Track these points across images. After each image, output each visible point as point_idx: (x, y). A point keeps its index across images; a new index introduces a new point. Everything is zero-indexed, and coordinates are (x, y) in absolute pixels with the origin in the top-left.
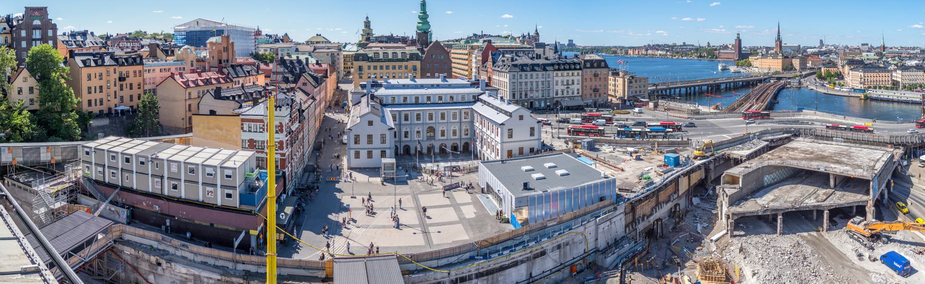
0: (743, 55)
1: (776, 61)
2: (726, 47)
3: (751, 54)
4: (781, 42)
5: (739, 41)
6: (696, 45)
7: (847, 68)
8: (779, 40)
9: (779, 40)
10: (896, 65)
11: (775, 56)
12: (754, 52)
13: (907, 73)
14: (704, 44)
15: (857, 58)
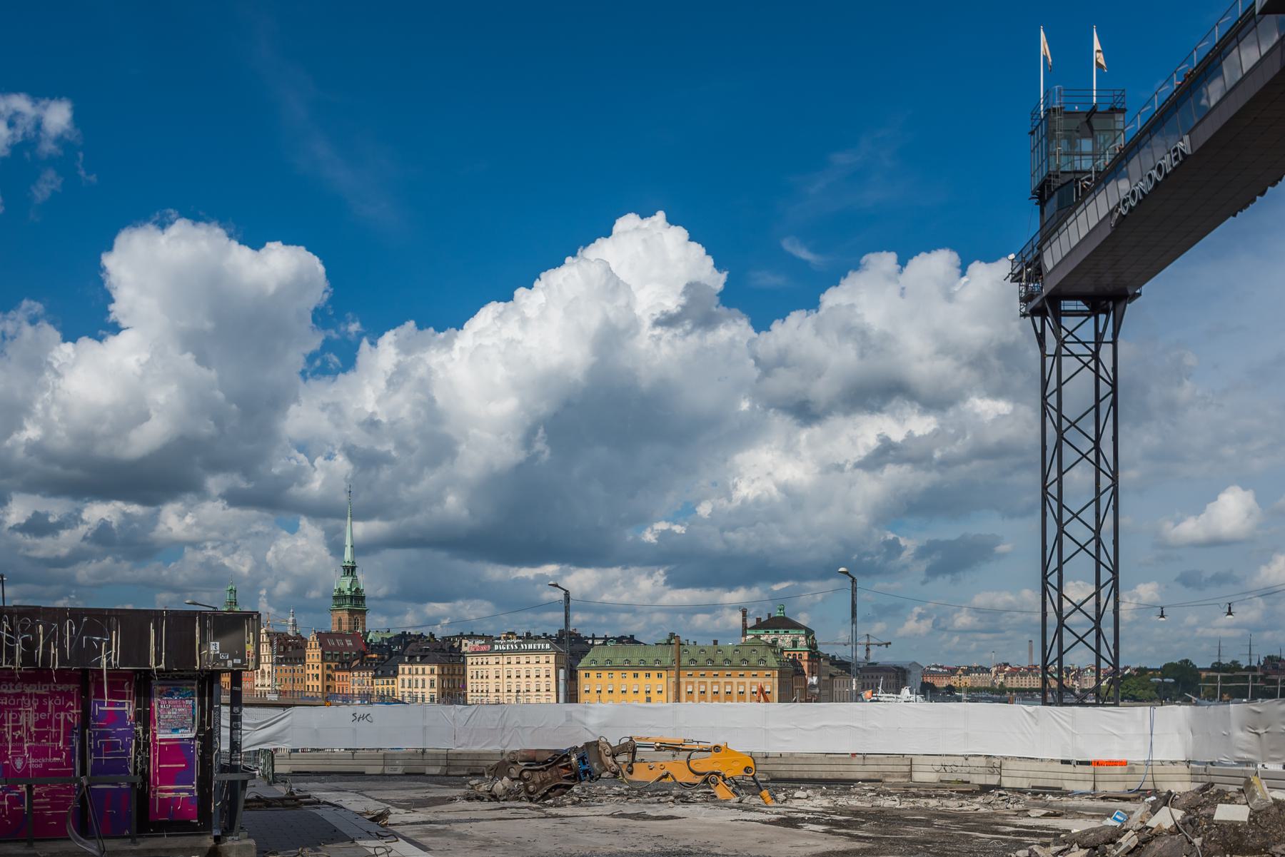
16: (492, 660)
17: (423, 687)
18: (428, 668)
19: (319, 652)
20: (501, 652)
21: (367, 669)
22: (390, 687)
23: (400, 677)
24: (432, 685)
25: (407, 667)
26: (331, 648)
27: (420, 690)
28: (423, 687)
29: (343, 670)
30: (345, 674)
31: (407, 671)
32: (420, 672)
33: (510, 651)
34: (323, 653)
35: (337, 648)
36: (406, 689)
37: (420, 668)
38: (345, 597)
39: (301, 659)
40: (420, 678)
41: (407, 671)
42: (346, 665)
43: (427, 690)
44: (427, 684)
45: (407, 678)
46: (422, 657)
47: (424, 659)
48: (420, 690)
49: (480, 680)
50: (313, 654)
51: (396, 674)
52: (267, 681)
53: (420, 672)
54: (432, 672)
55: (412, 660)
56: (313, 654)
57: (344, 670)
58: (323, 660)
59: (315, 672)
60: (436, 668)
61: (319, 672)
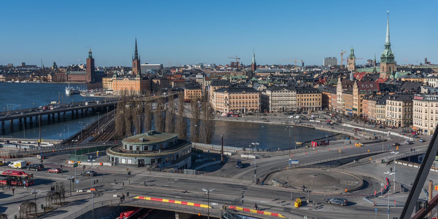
0: (97, 77)
1: (133, 82)
2: (76, 68)
3: (106, 76)
4: (139, 62)
5: (92, 61)
6: (39, 65)
7: (211, 89)
8: (137, 60)
9: (137, 60)
10: (265, 85)
11: (133, 76)
12: (108, 73)
13: (277, 93)
14: (50, 65)
15: (224, 78)
16: (424, 104)
17: (396, 111)
18: (398, 103)
19: (357, 90)
20: (429, 101)
21: (374, 100)
22: (383, 109)
23: (387, 105)
24: (400, 111)
25: (390, 101)
26: (363, 89)
27: (394, 112)
28: (396, 111)
29: (365, 99)
30: (366, 101)
31: (389, 103)
32: (395, 104)
33: (433, 101)
34: (359, 90)
35: (366, 88)
36: (389, 111)
37: (395, 102)
38: (385, 58)
39: (351, 92)
40: (395, 107)
41: (389, 103)
42: (367, 97)
43: (398, 112)
44: (398, 110)
45: (390, 106)
46: (396, 98)
47: (397, 99)
48: (394, 112)
49: (418, 113)
50: (355, 90)
51: (385, 104)
52: (341, 99)
53: (395, 104)
54: (400, 105)
55: (392, 99)
56: (355, 90)
57: (366, 99)
58: (359, 93)
59: (356, 98)
60: (402, 103)
61: (357, 98)
